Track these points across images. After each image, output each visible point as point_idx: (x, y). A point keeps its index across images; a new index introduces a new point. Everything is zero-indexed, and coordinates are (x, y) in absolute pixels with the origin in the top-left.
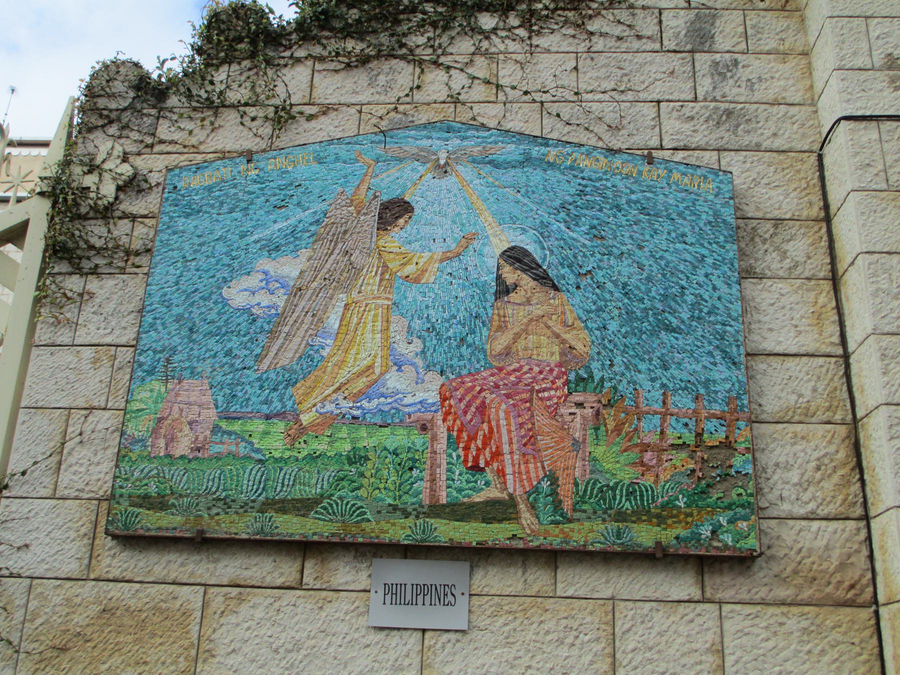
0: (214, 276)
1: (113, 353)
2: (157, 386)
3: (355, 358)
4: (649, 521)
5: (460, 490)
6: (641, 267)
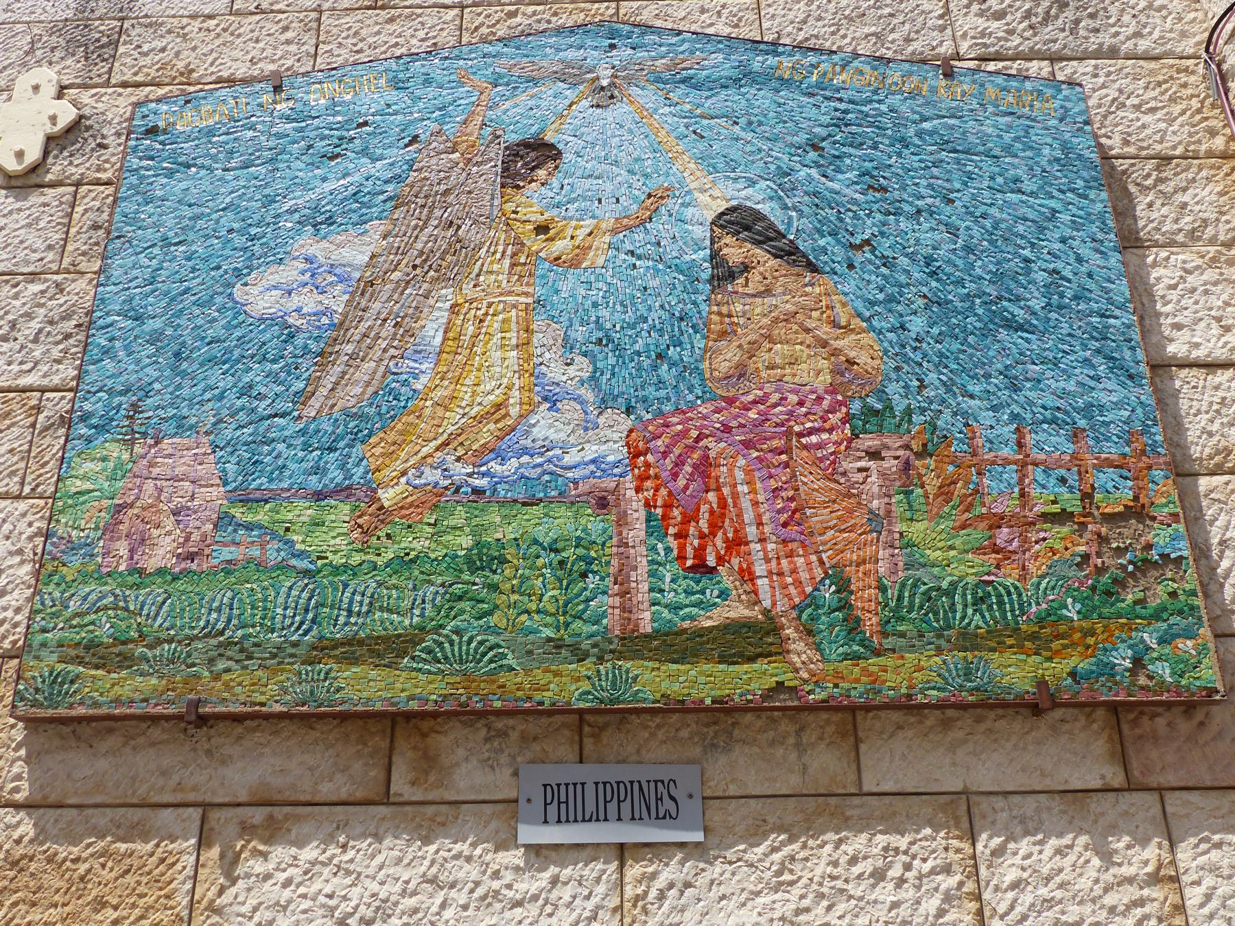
0: (218, 268)
1: (34, 402)
2: (116, 451)
3: (474, 392)
4: (1021, 648)
5: (675, 608)
6: (953, 231)
